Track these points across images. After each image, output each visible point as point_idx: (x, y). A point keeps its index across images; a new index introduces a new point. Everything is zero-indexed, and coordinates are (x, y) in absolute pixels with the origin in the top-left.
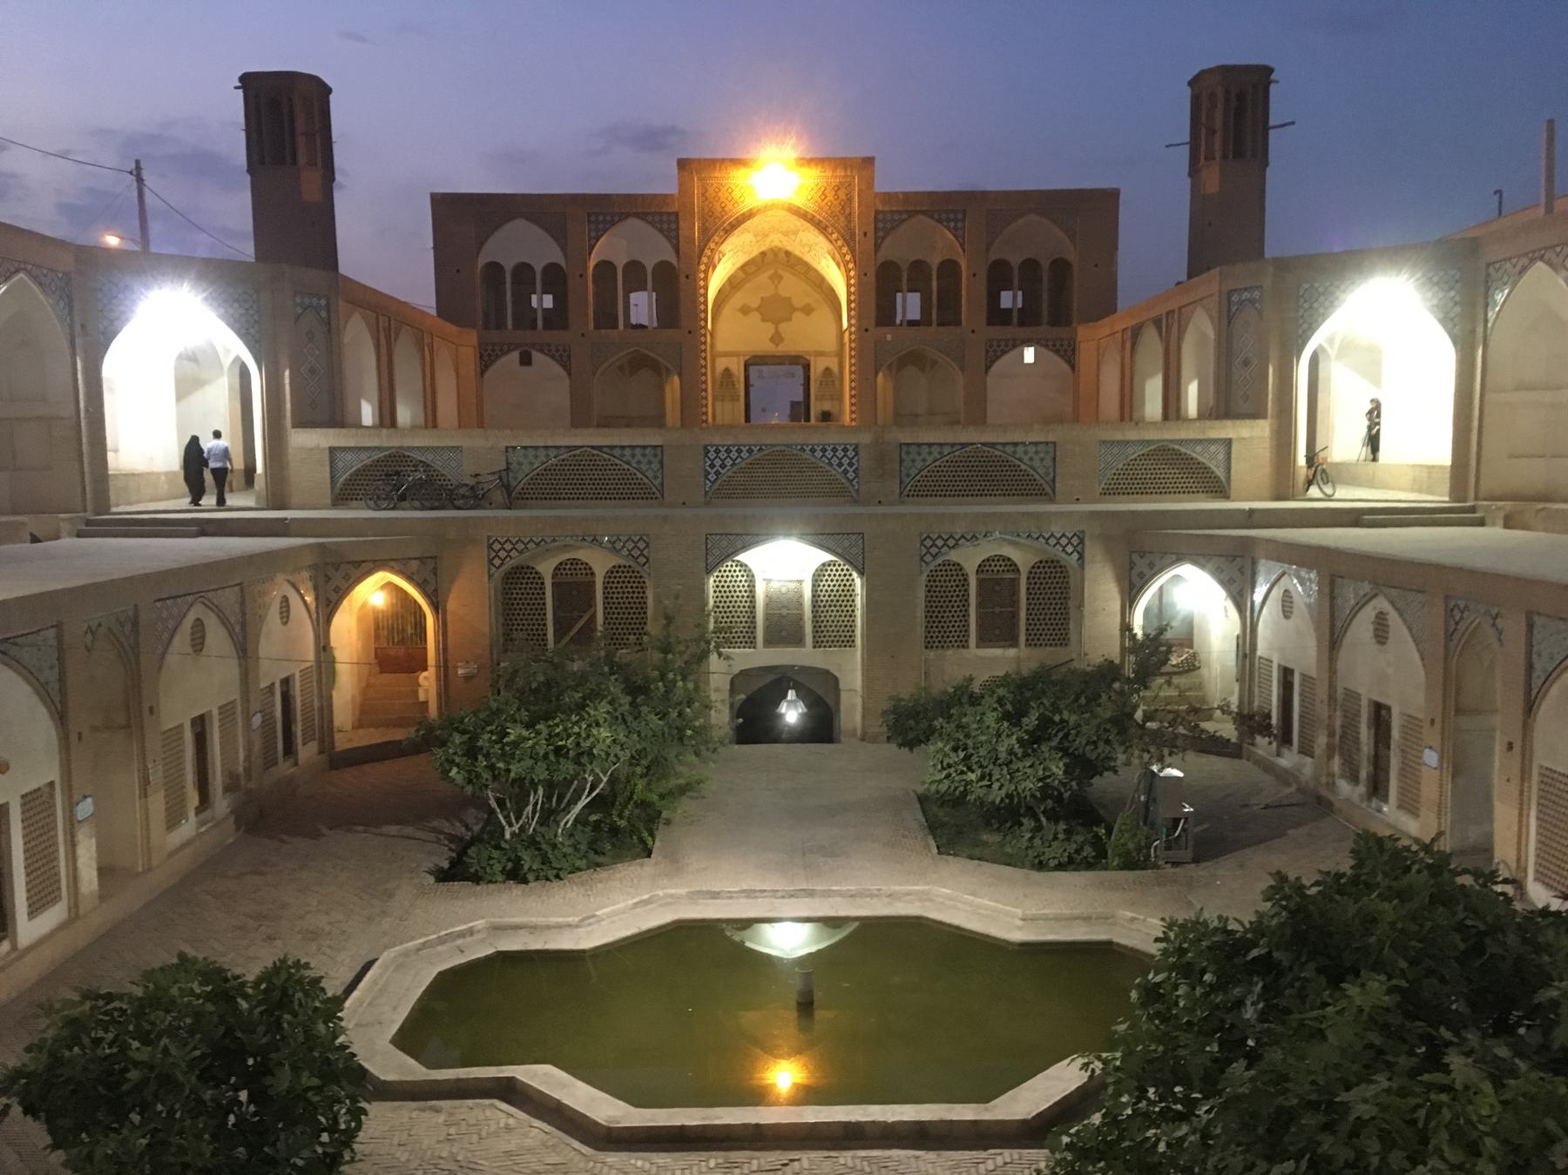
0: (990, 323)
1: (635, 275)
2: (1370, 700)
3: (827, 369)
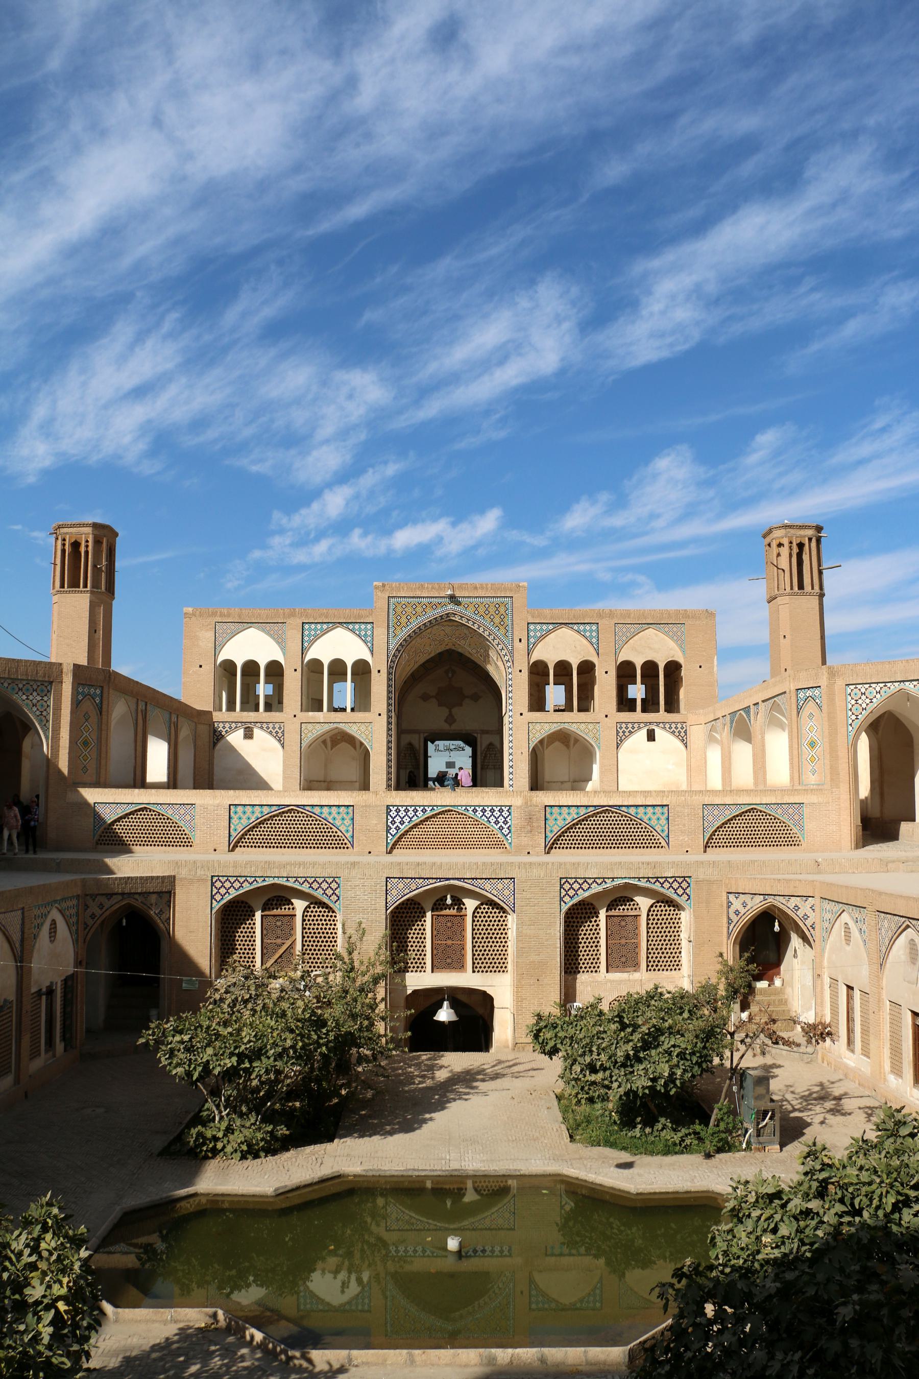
0: (620, 709)
2: (466, 971)
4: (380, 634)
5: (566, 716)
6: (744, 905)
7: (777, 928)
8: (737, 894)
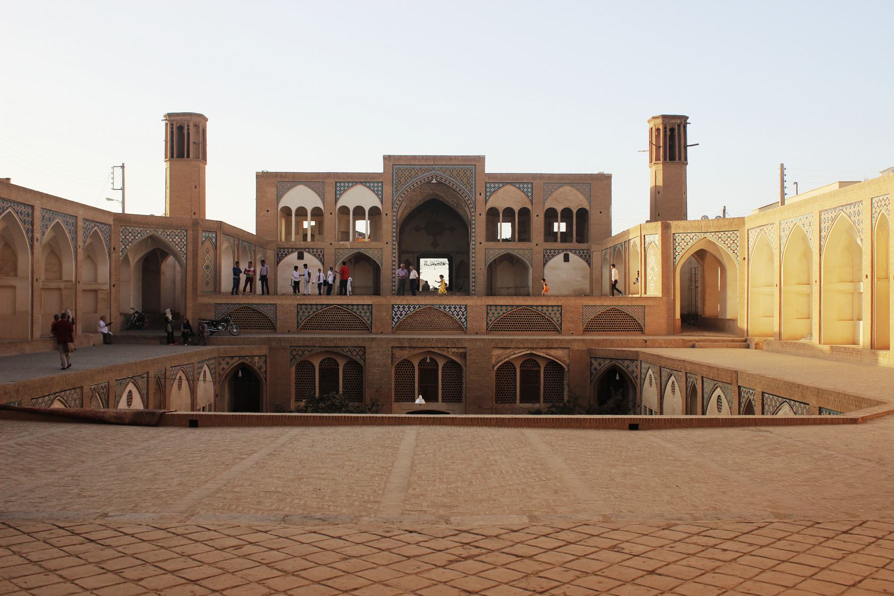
0: (546, 241)
1: (359, 212)
3: (462, 261)
4: (388, 190)
5: (511, 245)
6: (600, 364)
7: (617, 378)
8: (596, 358)
